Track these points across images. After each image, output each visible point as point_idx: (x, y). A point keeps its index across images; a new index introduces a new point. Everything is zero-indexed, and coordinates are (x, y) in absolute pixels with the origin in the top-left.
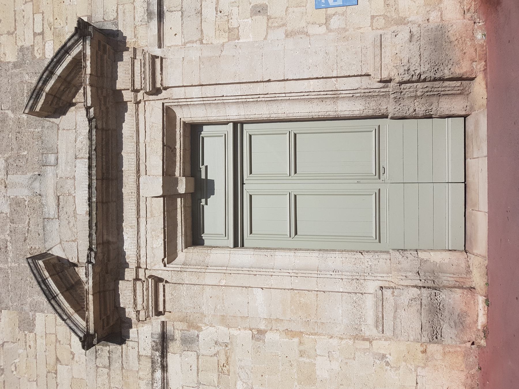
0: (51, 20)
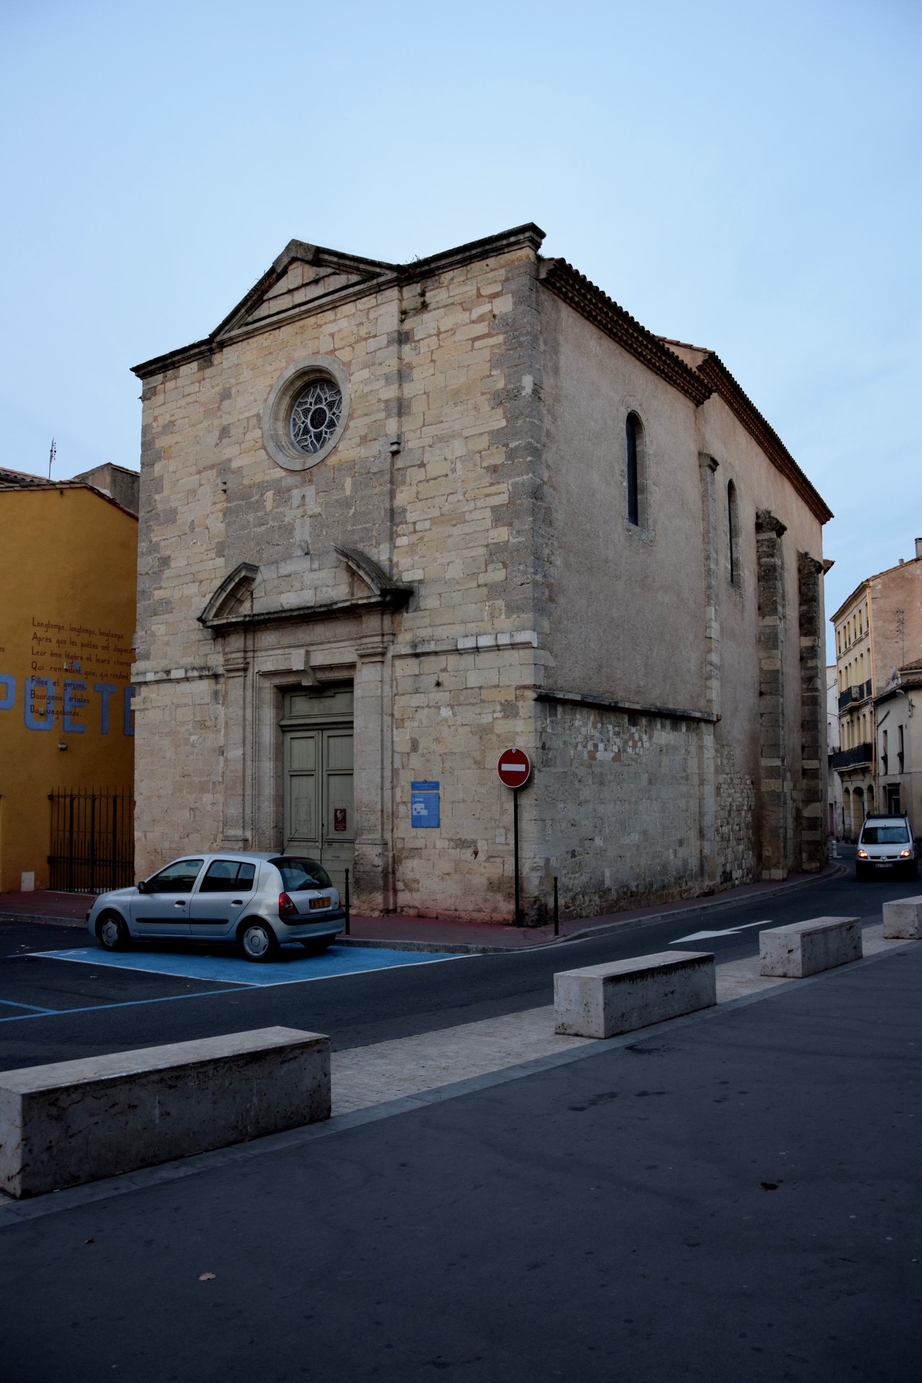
0: (425, 539)
